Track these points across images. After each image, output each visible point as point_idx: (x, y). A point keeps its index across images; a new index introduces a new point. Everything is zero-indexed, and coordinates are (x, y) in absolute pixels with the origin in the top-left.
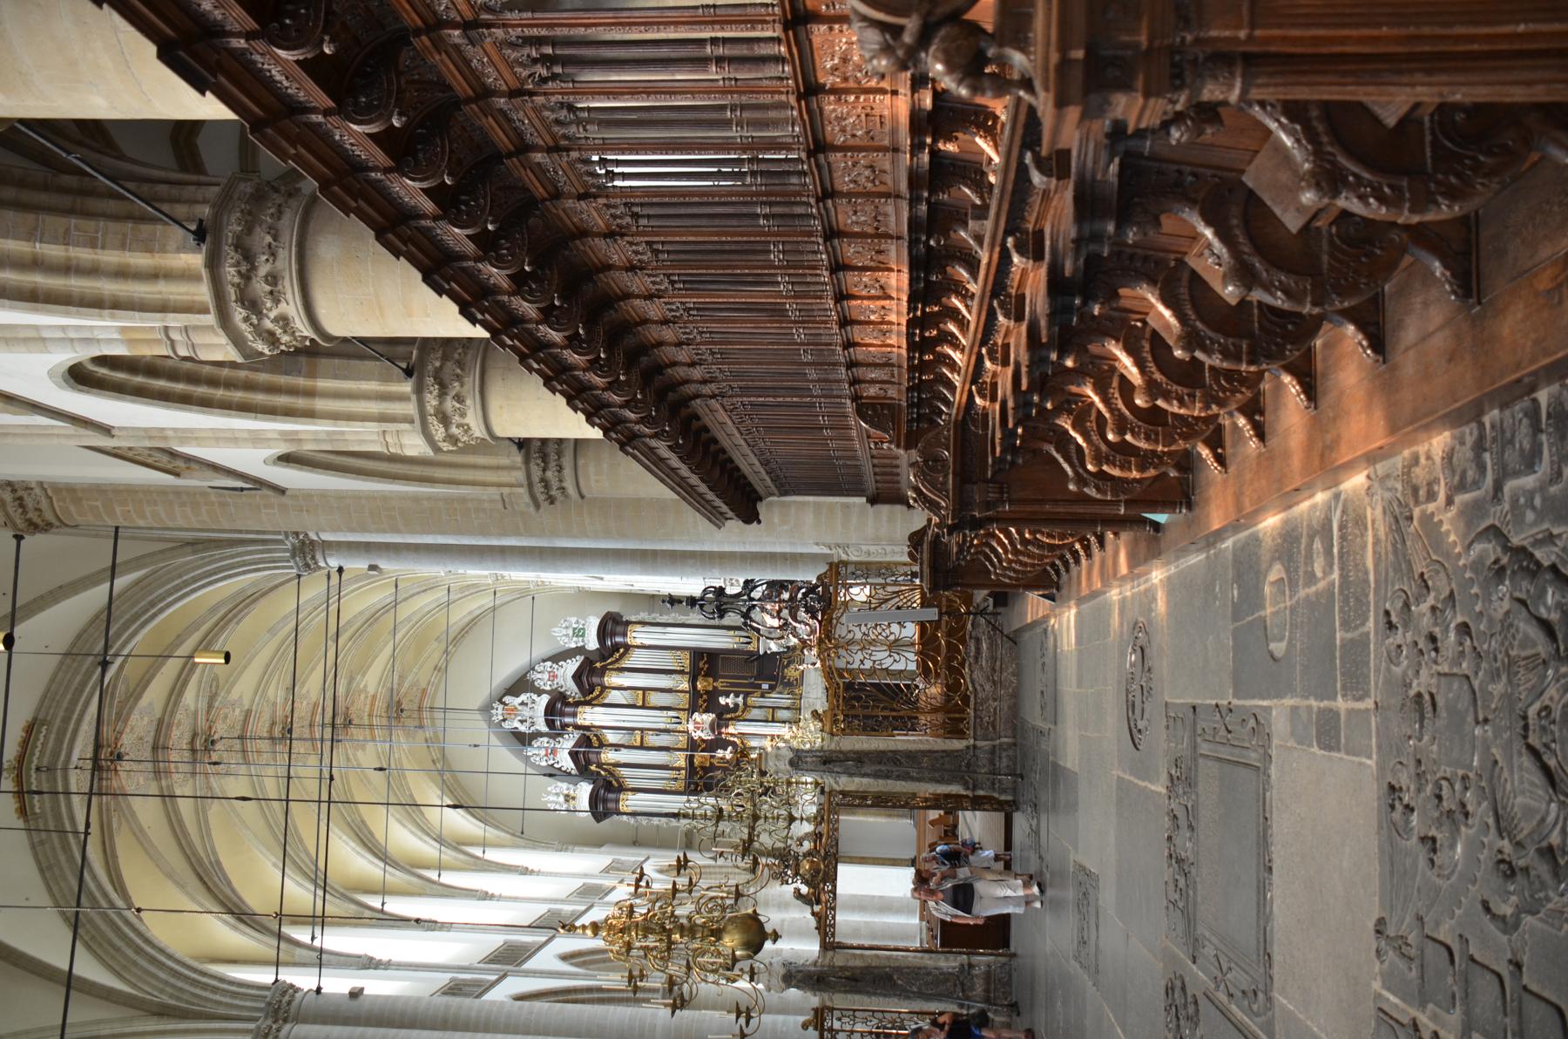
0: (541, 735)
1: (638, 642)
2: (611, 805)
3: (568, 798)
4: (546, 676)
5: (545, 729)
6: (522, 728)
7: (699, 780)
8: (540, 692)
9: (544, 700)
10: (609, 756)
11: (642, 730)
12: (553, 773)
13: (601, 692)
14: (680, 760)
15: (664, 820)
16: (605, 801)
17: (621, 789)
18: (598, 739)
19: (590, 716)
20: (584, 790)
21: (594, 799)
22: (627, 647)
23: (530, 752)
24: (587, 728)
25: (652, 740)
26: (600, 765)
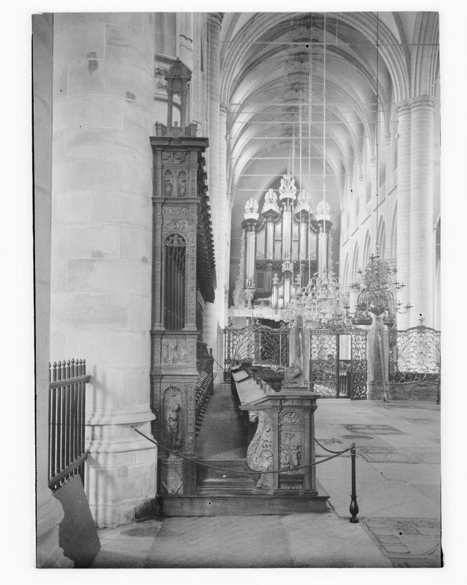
1: (320, 237)
2: (249, 227)
4: (304, 197)
5: (281, 198)
6: (281, 188)
7: (260, 266)
8: (297, 195)
9: (294, 198)
10: (270, 226)
11: (282, 241)
12: (262, 202)
13: (297, 222)
14: (271, 258)
16: (251, 226)
17: (257, 232)
18: (277, 222)
19: (287, 217)
20: (255, 216)
21: (251, 221)
22: (317, 233)
24: (282, 216)
25: (278, 245)
26: (266, 222)
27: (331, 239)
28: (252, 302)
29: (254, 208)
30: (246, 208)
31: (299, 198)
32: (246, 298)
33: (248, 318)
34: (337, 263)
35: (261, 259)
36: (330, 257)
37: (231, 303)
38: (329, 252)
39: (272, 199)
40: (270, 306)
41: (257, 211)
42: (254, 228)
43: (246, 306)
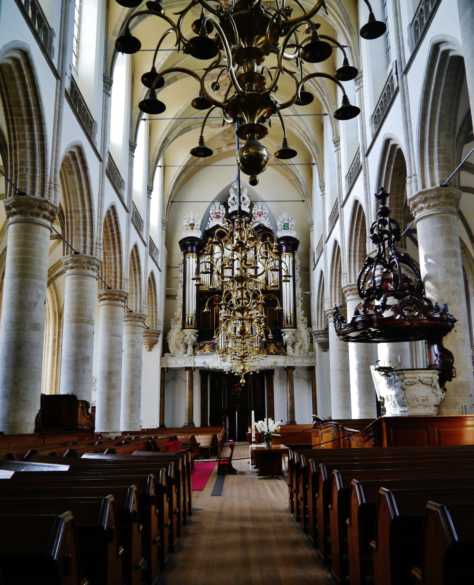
0: (227, 210)
2: (190, 248)
3: (192, 225)
4: (260, 210)
5: (230, 211)
6: (230, 199)
8: (251, 207)
15: (182, 279)
16: (192, 245)
20: (198, 234)
22: (279, 254)
23: (218, 204)
27: (298, 262)
28: (194, 347)
29: (195, 224)
30: (185, 223)
31: (253, 212)
32: (185, 341)
33: (187, 369)
34: (307, 293)
35: (206, 289)
36: (298, 284)
37: (165, 349)
38: (296, 278)
39: (219, 213)
40: (217, 351)
41: (199, 227)
42: (195, 249)
43: (186, 353)
